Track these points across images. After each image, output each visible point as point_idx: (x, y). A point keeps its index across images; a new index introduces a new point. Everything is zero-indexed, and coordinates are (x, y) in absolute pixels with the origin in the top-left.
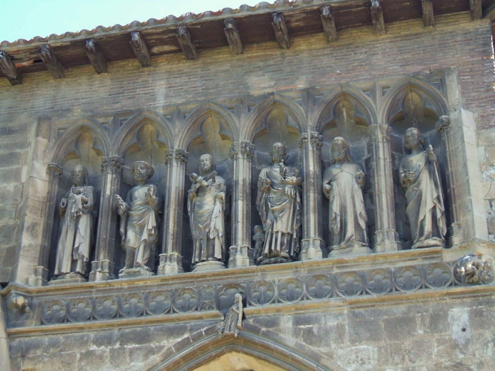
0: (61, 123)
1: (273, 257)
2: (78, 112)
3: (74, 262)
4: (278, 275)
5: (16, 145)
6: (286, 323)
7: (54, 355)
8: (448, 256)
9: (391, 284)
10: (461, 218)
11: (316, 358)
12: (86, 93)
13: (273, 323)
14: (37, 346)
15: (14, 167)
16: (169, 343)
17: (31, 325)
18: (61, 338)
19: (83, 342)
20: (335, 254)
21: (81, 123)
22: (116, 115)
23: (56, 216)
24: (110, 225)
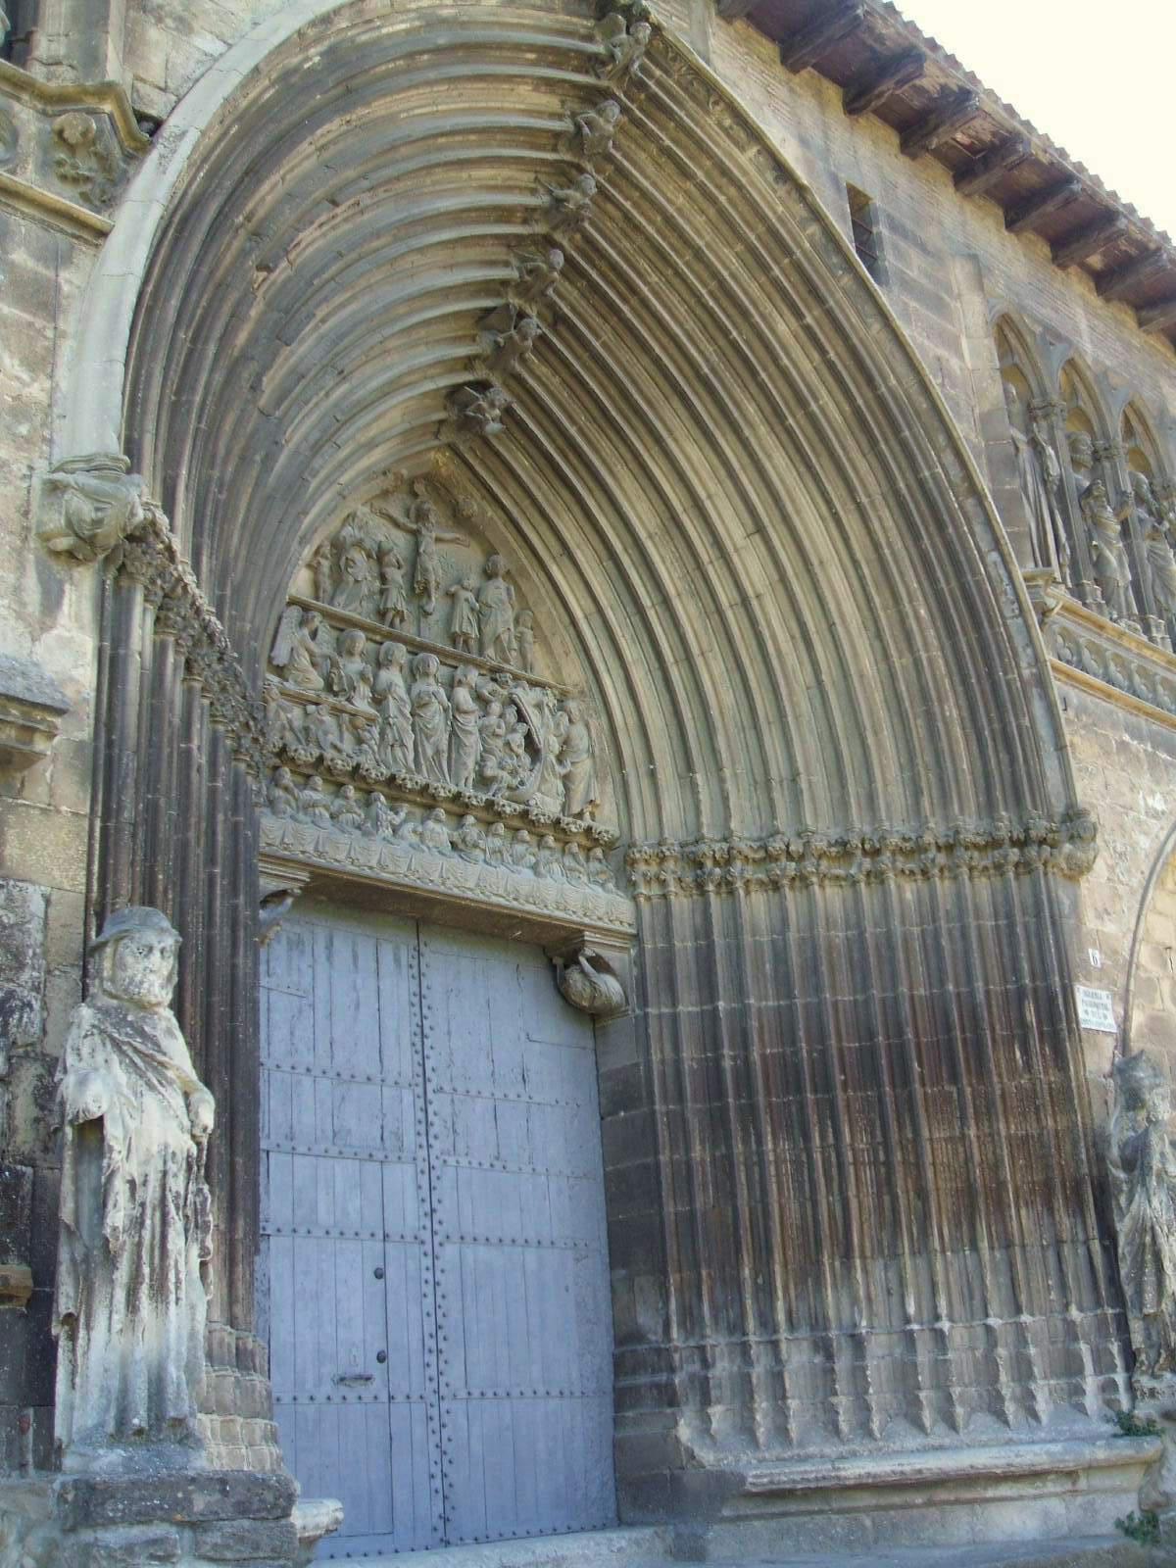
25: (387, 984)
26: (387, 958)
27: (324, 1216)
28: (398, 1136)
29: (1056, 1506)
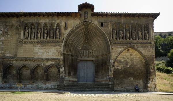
1: (134, 40)
2: (114, 22)
4: (135, 41)
6: (135, 46)
8: (149, 41)
9: (144, 43)
10: (150, 38)
11: (138, 49)
12: (114, 19)
13: (134, 46)
16: (126, 47)
19: (118, 46)
20: (139, 40)
23: (113, 32)
24: (118, 34)
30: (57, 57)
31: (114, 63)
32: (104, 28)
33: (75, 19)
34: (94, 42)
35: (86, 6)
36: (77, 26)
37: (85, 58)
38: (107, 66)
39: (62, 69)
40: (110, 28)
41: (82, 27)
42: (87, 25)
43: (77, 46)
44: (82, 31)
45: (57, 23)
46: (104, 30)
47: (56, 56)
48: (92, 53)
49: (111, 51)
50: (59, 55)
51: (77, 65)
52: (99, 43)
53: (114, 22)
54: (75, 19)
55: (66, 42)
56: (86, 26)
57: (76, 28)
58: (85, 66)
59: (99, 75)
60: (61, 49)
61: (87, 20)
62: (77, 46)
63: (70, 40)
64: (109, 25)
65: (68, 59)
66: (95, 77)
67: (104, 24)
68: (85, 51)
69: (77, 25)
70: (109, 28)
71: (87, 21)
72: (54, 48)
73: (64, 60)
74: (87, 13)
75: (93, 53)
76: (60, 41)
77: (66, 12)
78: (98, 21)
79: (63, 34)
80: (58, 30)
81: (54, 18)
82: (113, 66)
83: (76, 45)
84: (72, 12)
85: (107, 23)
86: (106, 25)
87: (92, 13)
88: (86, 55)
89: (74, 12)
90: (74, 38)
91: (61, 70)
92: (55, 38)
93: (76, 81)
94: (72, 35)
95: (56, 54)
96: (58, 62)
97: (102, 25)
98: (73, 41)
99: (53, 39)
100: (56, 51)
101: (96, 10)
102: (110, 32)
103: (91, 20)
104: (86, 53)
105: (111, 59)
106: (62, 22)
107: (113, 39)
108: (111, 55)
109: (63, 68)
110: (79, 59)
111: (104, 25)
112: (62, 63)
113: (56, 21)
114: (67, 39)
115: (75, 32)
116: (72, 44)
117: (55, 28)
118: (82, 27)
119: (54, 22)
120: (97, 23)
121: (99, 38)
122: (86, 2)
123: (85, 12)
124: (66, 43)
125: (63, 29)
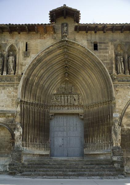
0: (115, 43)
2: (118, 41)
3: (122, 71)
5: (106, 46)
7: (122, 87)
14: (118, 86)
15: (107, 51)
17: (116, 82)
18: (123, 85)
21: (119, 43)
22: (126, 42)
25: (64, 120)
26: (64, 117)
27: (59, 136)
28: (65, 130)
29: (105, 157)
30: (9, 109)
31: (121, 118)
32: (100, 53)
33: (45, 38)
34: (81, 79)
35: (65, 12)
36: (47, 50)
37: (65, 110)
38: (107, 124)
39: (18, 131)
40: (111, 52)
41: (58, 52)
42: (67, 48)
43: (49, 87)
44: (57, 60)
45: (9, 45)
46: (100, 57)
47: (8, 106)
48: (77, 99)
49: (114, 96)
50: (13, 105)
51: (48, 124)
52: (90, 81)
53: (118, 41)
54: (45, 38)
55: (27, 81)
56: (65, 50)
57: (46, 53)
58: (65, 125)
59: (92, 142)
60: (16, 93)
61: (67, 39)
62: (49, 87)
63: (35, 75)
64: (108, 46)
65: (31, 112)
66: (84, 146)
67: (100, 46)
68: (64, 97)
69: (49, 48)
70: (110, 52)
71: (67, 41)
72: (3, 91)
73: (22, 114)
74: (67, 25)
75: (79, 99)
76: (15, 77)
77: (26, 25)
78: (88, 40)
79: (22, 65)
80: (11, 59)
81: (5, 36)
82: (120, 125)
83: (46, 86)
84: (38, 24)
85: (105, 43)
86: (103, 47)
87: (76, 24)
88: (66, 104)
89: (42, 24)
90: (42, 71)
91: (17, 134)
92: (5, 73)
93: (47, 155)
94: (38, 67)
95: (8, 103)
96: (11, 118)
97: (96, 47)
98: (41, 78)
99: (2, 74)
100: (7, 96)
101: (83, 21)
102: (111, 60)
103: (75, 39)
104: (66, 100)
105: (115, 112)
106: (19, 42)
107: (118, 73)
108: (115, 104)
109: (21, 130)
110: (53, 111)
111: (99, 47)
112: (18, 120)
113: (7, 41)
114: (28, 74)
115: (44, 61)
116: (38, 84)
117: (5, 53)
118: (58, 52)
119: (3, 42)
120: (87, 44)
121: (90, 71)
122: (65, 5)
123: (63, 24)
124: (27, 82)
125: (21, 55)
